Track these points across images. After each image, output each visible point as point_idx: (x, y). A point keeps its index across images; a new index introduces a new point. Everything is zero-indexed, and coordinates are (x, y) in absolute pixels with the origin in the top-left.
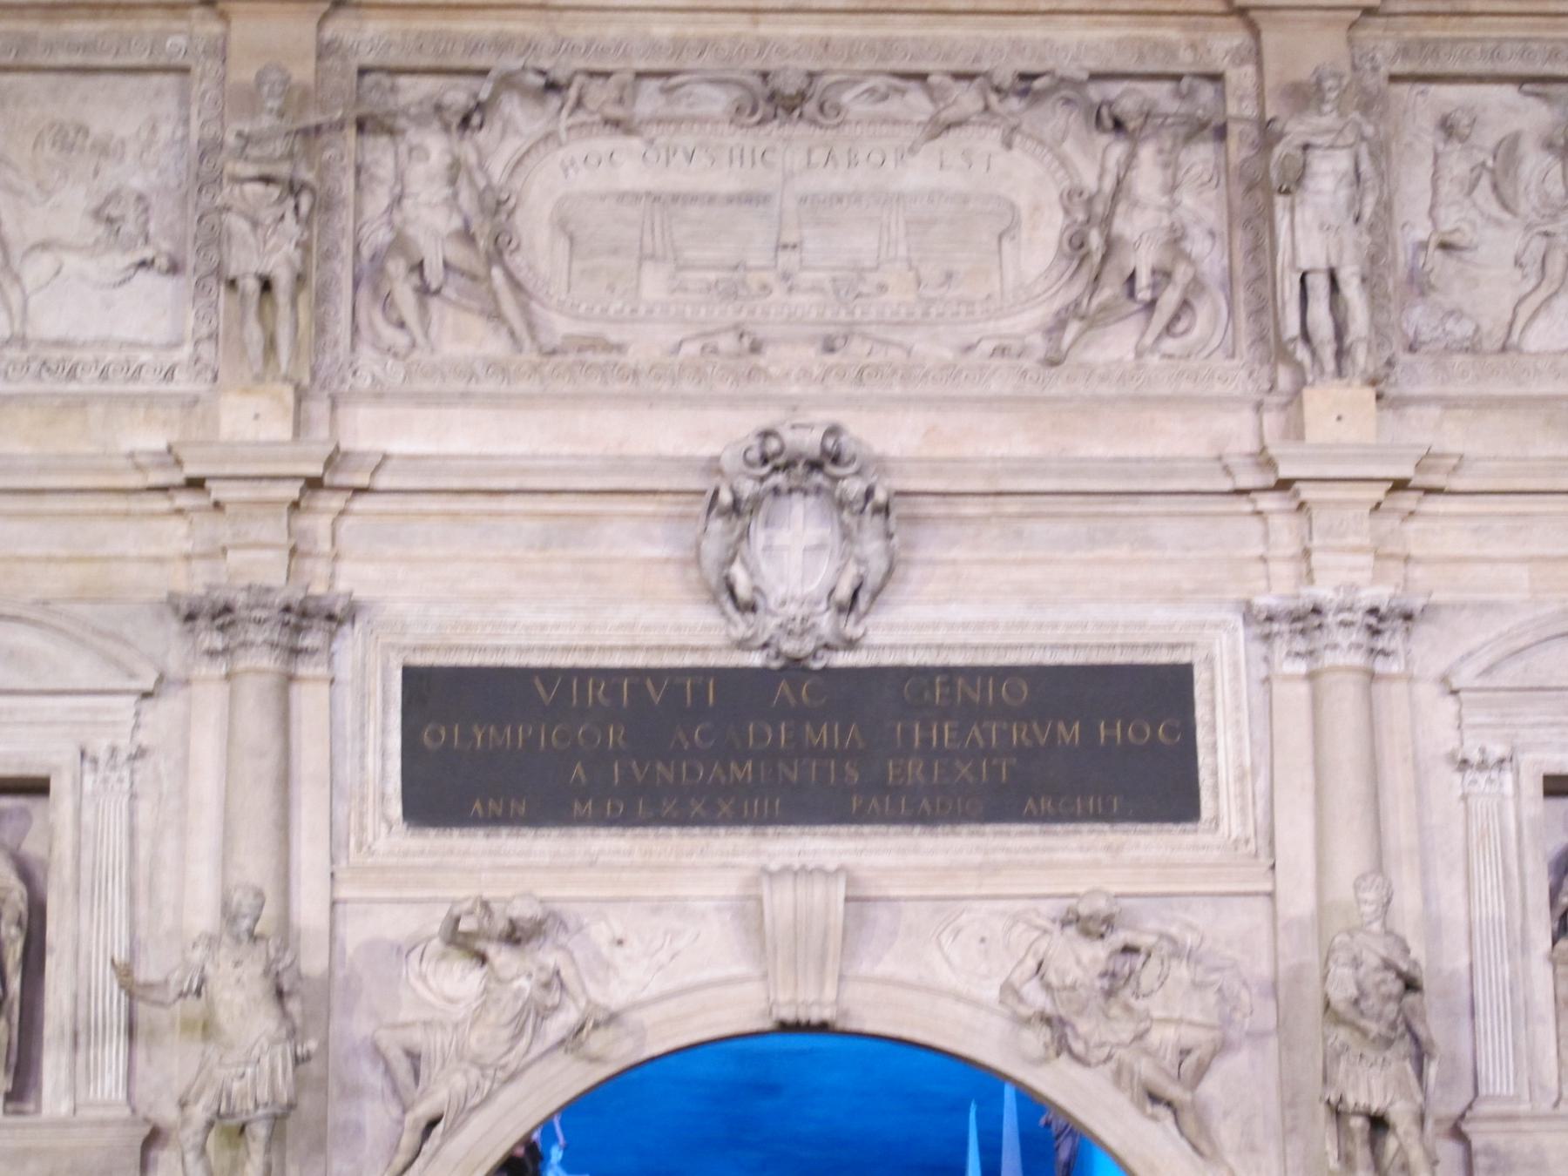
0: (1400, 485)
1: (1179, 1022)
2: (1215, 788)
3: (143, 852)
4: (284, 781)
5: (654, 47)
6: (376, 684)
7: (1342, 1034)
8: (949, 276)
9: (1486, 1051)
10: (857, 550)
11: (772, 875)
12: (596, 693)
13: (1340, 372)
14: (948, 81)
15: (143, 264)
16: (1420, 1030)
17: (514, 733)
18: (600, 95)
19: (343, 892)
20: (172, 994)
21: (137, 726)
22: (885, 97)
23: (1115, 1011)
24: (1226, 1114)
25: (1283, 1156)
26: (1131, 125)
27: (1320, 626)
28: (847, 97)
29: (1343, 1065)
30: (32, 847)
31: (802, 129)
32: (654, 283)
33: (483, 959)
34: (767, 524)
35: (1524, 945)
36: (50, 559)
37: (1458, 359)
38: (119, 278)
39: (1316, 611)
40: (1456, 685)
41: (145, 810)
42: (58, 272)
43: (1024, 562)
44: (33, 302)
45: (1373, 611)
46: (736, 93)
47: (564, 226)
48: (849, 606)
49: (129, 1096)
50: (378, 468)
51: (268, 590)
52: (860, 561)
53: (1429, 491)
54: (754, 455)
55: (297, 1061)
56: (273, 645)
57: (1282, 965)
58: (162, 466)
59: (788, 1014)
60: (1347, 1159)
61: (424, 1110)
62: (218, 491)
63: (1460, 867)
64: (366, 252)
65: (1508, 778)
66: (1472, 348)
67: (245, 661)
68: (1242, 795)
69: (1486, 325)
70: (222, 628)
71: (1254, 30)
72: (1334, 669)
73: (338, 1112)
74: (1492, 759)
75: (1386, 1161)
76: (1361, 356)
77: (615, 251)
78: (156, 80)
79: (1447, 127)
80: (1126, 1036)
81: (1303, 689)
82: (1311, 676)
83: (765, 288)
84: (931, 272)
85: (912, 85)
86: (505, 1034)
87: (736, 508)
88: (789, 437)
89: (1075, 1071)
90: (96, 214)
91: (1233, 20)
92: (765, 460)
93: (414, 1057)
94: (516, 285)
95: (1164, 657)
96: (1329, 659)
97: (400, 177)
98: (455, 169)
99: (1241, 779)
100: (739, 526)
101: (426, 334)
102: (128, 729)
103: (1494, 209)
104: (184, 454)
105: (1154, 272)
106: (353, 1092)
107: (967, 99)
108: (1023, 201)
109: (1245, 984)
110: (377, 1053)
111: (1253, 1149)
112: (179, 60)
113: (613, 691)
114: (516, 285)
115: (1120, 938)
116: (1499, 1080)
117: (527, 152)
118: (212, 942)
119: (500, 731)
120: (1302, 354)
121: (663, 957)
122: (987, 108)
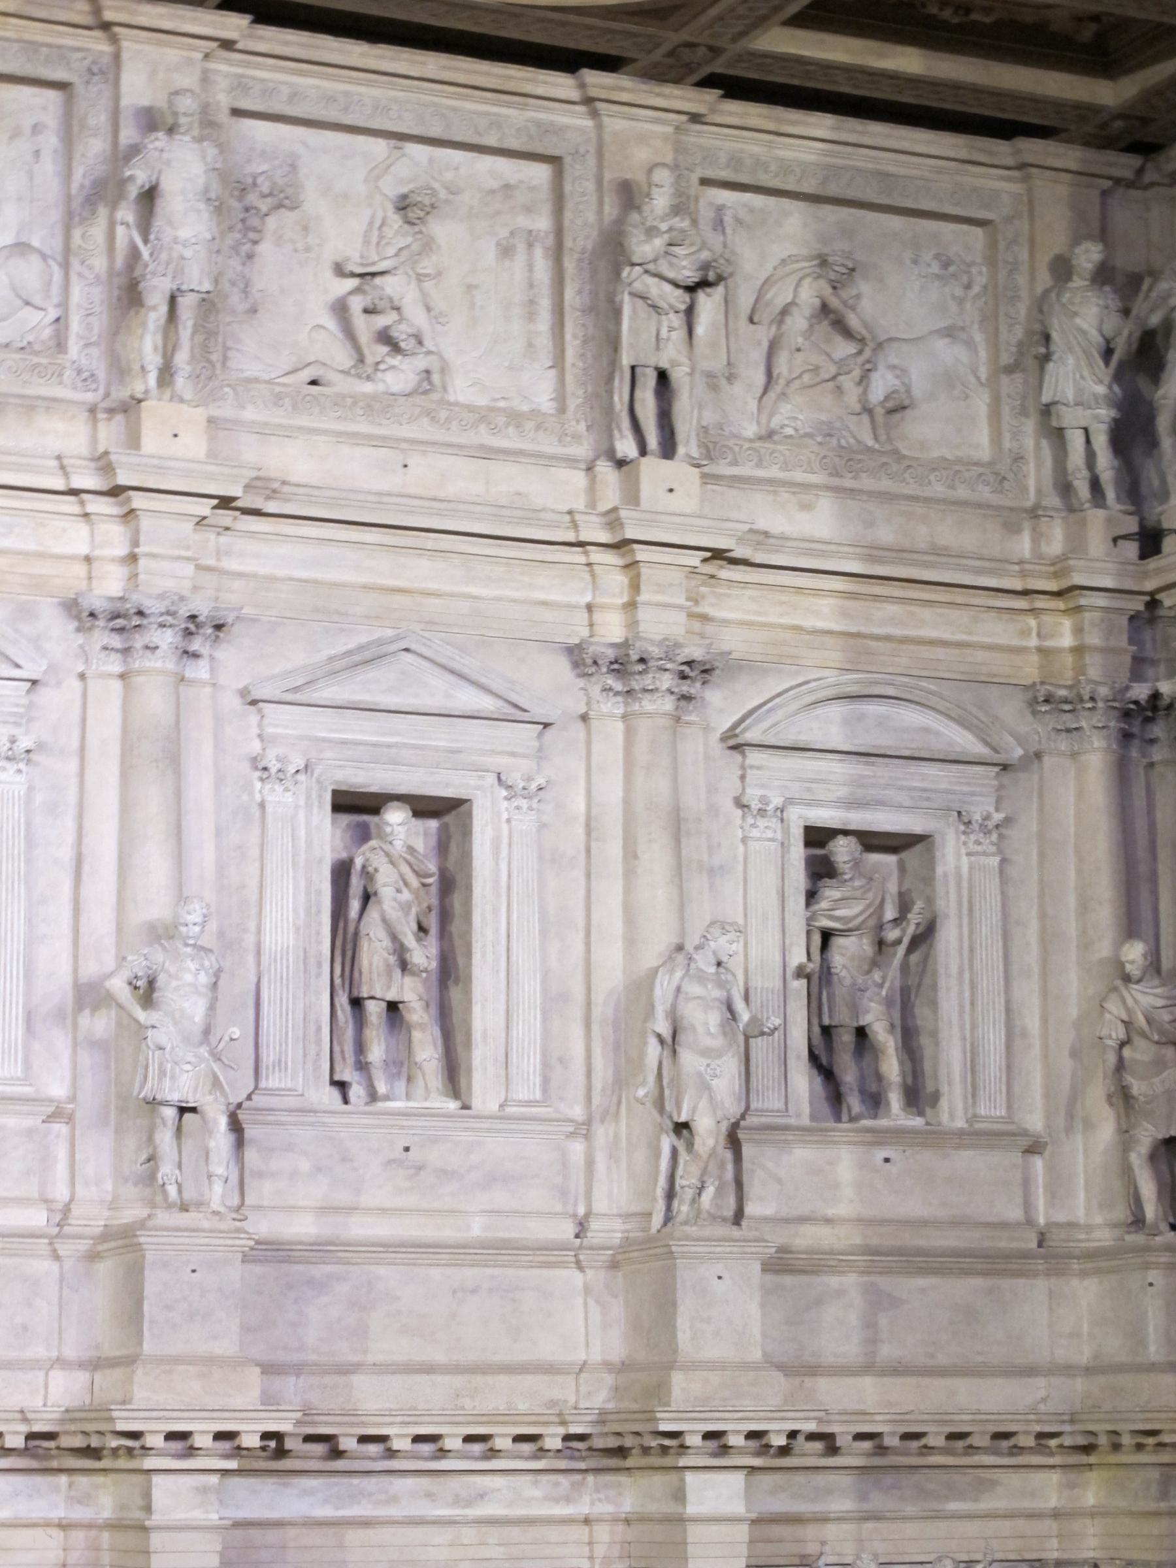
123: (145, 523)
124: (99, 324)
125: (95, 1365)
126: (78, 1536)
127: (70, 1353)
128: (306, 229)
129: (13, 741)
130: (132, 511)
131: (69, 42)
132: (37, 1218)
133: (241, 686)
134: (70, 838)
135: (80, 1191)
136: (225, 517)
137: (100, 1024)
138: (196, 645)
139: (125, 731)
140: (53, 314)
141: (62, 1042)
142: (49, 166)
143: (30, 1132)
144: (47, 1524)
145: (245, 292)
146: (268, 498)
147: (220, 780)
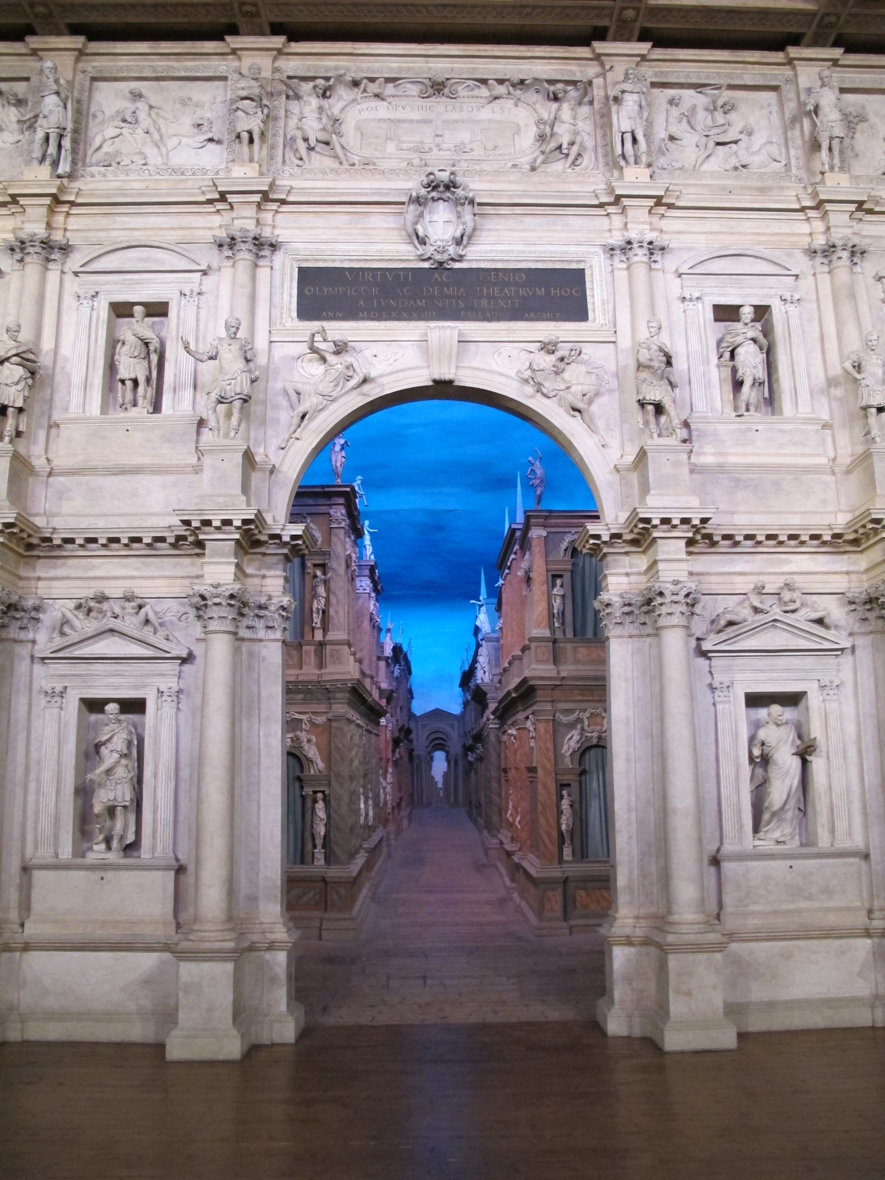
0: (659, 201)
1: (582, 384)
2: (594, 311)
3: (202, 327)
4: (253, 298)
5: (391, 70)
6: (288, 271)
7: (644, 375)
8: (496, 147)
9: (695, 396)
10: (462, 219)
11: (431, 329)
12: (369, 277)
13: (636, 163)
14: (495, 83)
15: (211, 140)
16: (672, 379)
17: (338, 290)
18: (373, 88)
19: (273, 339)
20: (206, 358)
21: (200, 284)
22: (473, 90)
23: (558, 379)
24: (600, 418)
25: (622, 431)
26: (560, 96)
27: (630, 249)
28: (460, 89)
29: (645, 385)
30: (163, 334)
31: (444, 99)
32: (391, 148)
33: (324, 360)
34: (430, 213)
35: (708, 361)
36: (171, 228)
37: (677, 172)
38: (201, 145)
39: (629, 243)
40: (681, 271)
41: (203, 312)
42: (179, 144)
43: (523, 230)
44: (171, 153)
45: (651, 243)
46: (420, 87)
47: (358, 128)
48: (459, 242)
49: (193, 409)
50: (289, 192)
51: (248, 231)
52: (464, 224)
53: (670, 206)
54: (425, 182)
55: (253, 381)
56: (250, 250)
57: (620, 364)
58: (211, 192)
59: (437, 377)
60: (646, 423)
61: (301, 409)
62: (231, 198)
63: (684, 335)
64: (289, 137)
65: (700, 305)
66: (681, 169)
67: (240, 255)
68: (604, 310)
69: (686, 165)
70: (231, 249)
71: (602, 65)
72: (637, 262)
73: (270, 414)
74: (694, 298)
75: (661, 425)
76: (644, 159)
77: (377, 137)
78: (216, 83)
79: (672, 102)
80: (563, 387)
81: (625, 273)
82: (628, 268)
83: (431, 149)
84: (490, 145)
85: (483, 86)
86: (332, 384)
87: (418, 201)
88: (437, 173)
89: (545, 400)
90: (194, 125)
91: (595, 62)
92: (429, 186)
93: (298, 394)
94: (343, 147)
95: (574, 266)
96: (635, 259)
97: (301, 113)
98: (321, 109)
99: (603, 304)
100: (420, 209)
101: (310, 161)
102: (197, 285)
103: (688, 128)
104: (218, 182)
105: (569, 144)
106: (276, 407)
107: (501, 90)
108: (522, 124)
109: (606, 373)
110: (286, 392)
111: (611, 430)
112: (224, 74)
113: (375, 276)
114: (343, 147)
115: (559, 354)
116: (700, 407)
117: (345, 106)
118: (220, 339)
119: (333, 289)
120: (622, 163)
121: (391, 361)
122: (509, 93)
123: (831, 216)
124: (801, 162)
125: (853, 511)
126: (854, 577)
127: (843, 507)
128: (872, 128)
129: (792, 296)
130: (826, 211)
131: (777, 72)
132: (824, 461)
133: (873, 275)
134: (817, 330)
135: (839, 451)
136: (859, 215)
137: (838, 392)
138: (855, 260)
139: (833, 290)
140: (784, 163)
141: (824, 400)
142: (775, 117)
143: (817, 431)
144: (841, 573)
145: (852, 150)
146: (876, 205)
147: (870, 308)
